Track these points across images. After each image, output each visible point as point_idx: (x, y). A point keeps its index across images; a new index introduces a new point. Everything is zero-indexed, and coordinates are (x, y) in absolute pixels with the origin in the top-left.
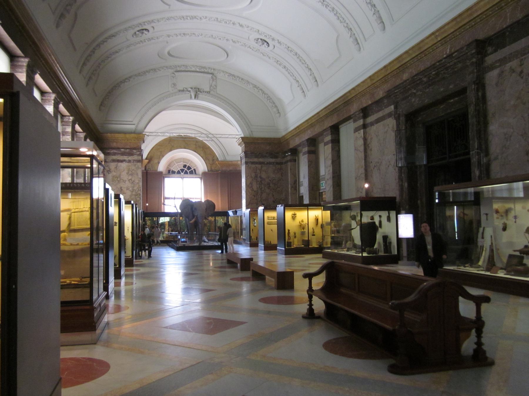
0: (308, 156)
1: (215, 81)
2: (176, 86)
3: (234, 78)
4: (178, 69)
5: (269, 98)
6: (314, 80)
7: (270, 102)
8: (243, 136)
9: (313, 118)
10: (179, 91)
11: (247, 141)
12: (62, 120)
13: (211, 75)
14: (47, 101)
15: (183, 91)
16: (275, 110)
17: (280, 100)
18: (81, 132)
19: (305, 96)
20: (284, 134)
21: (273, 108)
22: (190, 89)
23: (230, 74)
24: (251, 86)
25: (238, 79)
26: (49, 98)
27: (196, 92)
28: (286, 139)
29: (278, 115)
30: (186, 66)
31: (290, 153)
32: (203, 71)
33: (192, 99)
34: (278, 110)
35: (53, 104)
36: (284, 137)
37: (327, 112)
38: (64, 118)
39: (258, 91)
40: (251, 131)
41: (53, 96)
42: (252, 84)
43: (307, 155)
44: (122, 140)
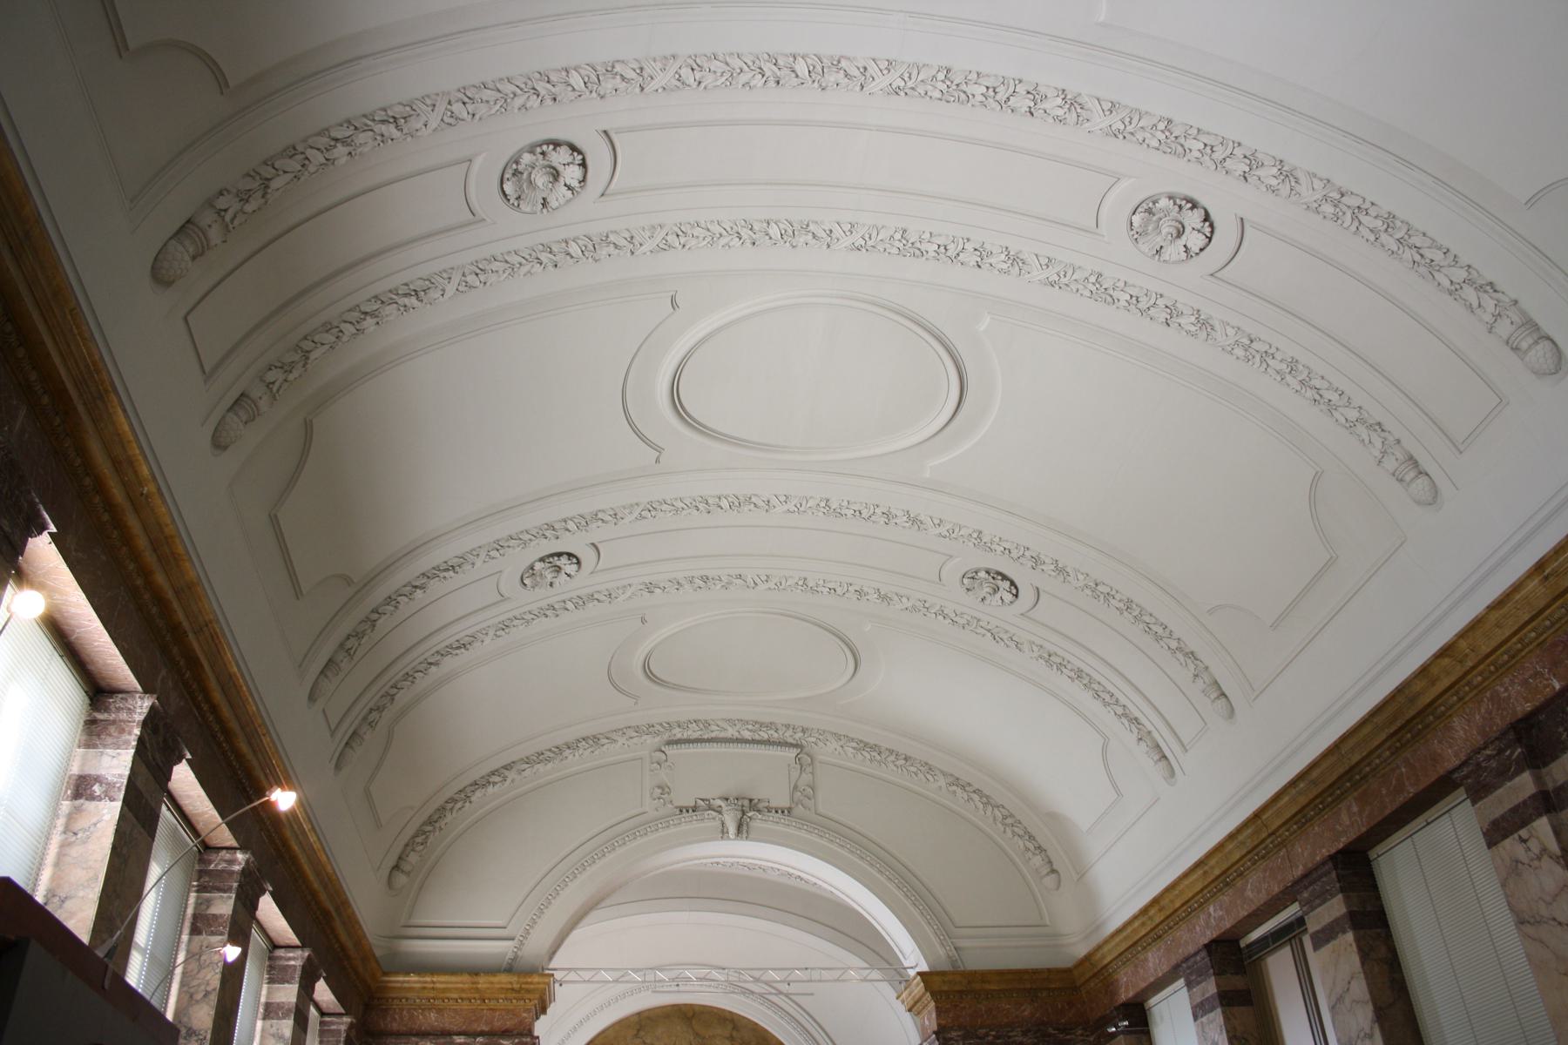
0: (1227, 1019)
1: (809, 769)
2: (669, 793)
3: (878, 758)
4: (678, 733)
5: (1009, 820)
6: (1156, 757)
7: (1013, 832)
8: (924, 968)
9: (1230, 846)
10: (681, 811)
11: (945, 988)
12: (203, 867)
13: (795, 751)
14: (112, 729)
15: (693, 811)
16: (1037, 860)
17: (1054, 819)
18: (297, 947)
19: (1172, 773)
20: (1081, 951)
21: (1030, 854)
22: (719, 802)
23: (862, 745)
24: (942, 782)
25: (892, 758)
26: (123, 716)
27: (744, 813)
28: (1099, 967)
29: (1050, 881)
30: (707, 724)
31: (1126, 1023)
32: (765, 738)
33: (729, 838)
34: (1050, 862)
35: (134, 743)
36: (1087, 958)
37: (1303, 800)
38: (213, 856)
39: (970, 799)
40: (955, 949)
41: (142, 705)
42: (944, 774)
43: (1219, 1010)
44: (462, 999)
